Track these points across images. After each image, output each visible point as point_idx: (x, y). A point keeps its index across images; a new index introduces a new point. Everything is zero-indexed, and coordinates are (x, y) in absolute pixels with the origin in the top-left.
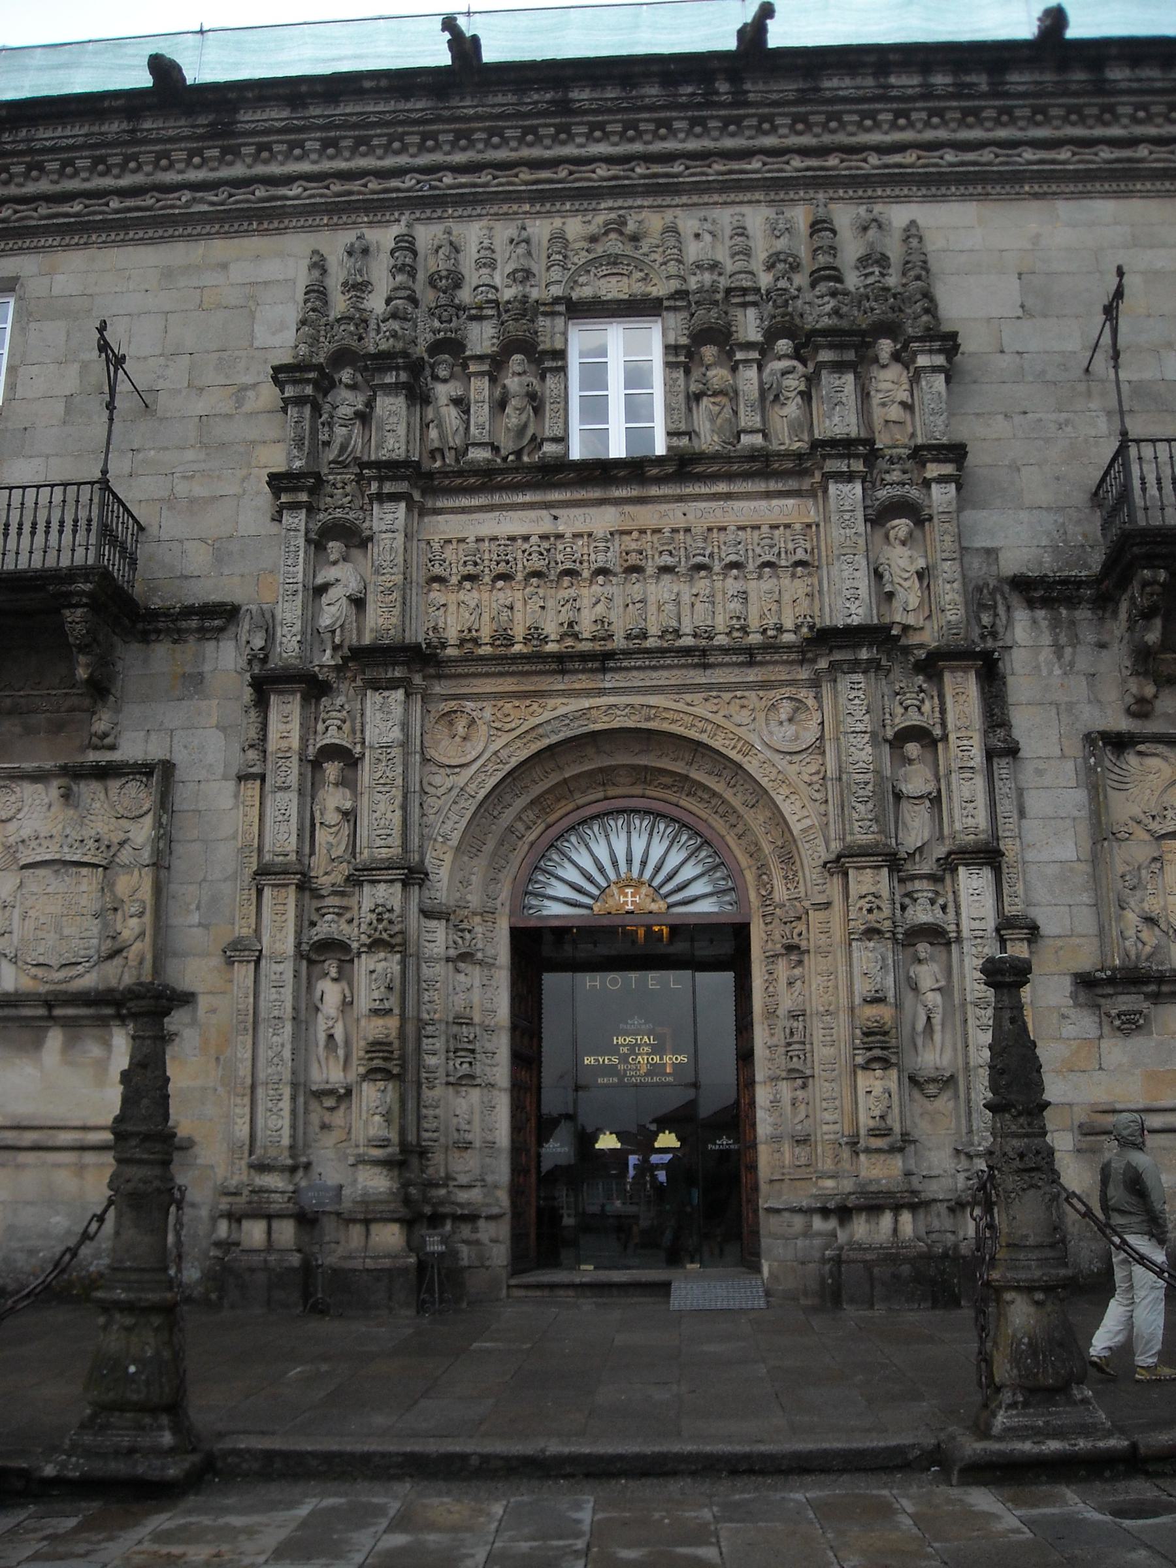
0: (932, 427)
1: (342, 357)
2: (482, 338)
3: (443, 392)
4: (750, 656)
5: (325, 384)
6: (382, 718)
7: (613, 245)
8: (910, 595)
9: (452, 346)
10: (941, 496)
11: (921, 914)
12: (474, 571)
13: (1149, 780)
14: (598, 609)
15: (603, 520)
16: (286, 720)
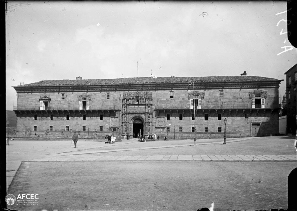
0: (151, 103)
1: (125, 99)
2: (131, 98)
3: (130, 100)
4: (142, 113)
5: (125, 100)
6: (127, 116)
7: (137, 93)
8: (149, 111)
9: (130, 98)
10: (151, 106)
11: (149, 124)
12: (130, 109)
13: (158, 119)
14: (137, 111)
15: (137, 107)
16: (123, 115)
